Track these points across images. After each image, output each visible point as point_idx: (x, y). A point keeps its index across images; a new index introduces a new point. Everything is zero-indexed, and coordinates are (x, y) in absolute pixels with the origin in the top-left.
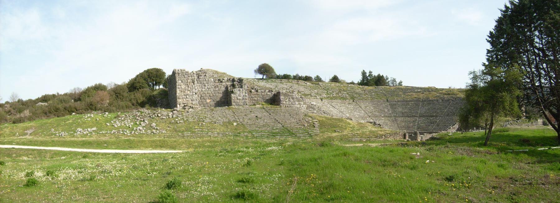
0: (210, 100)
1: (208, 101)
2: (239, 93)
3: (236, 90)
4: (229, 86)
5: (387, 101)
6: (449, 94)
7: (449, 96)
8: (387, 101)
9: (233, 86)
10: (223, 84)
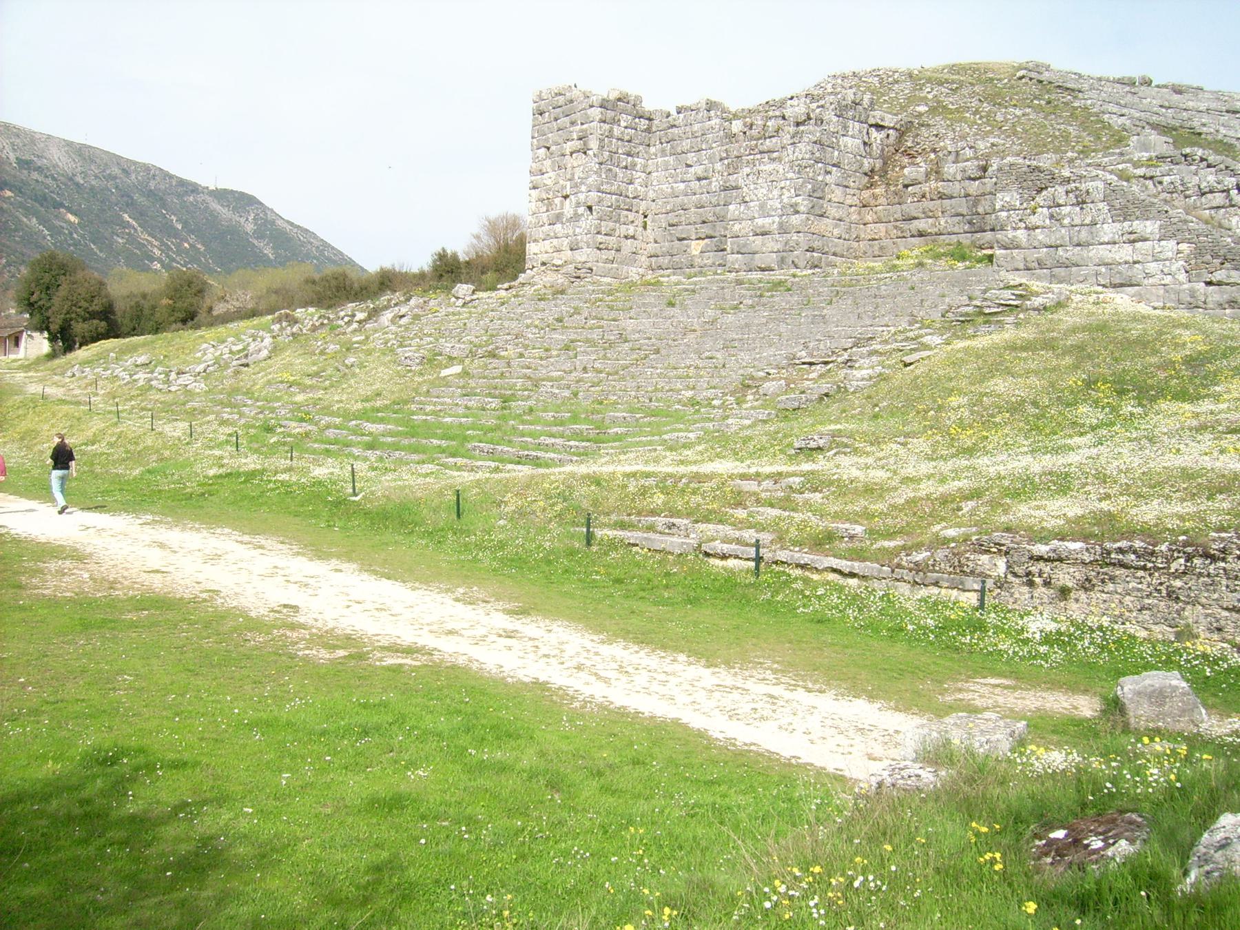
1: (696, 247)
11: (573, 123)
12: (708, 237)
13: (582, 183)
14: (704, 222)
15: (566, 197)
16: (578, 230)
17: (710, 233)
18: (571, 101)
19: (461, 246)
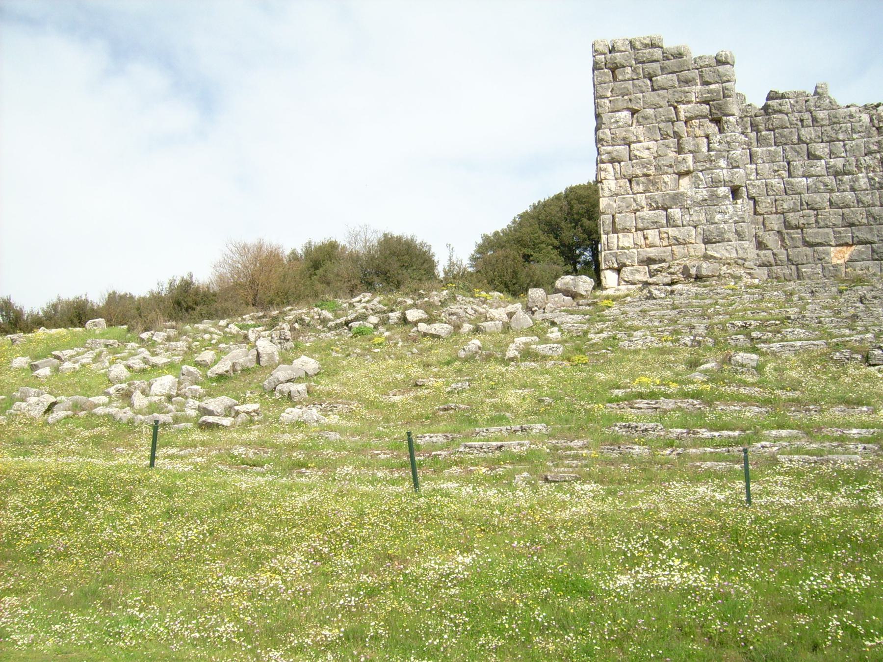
0: (848, 252)
1: (838, 256)
11: (687, 82)
12: (861, 243)
13: (718, 157)
14: (851, 225)
15: (681, 175)
16: (718, 217)
17: (869, 237)
18: (680, 55)
19: (204, 275)
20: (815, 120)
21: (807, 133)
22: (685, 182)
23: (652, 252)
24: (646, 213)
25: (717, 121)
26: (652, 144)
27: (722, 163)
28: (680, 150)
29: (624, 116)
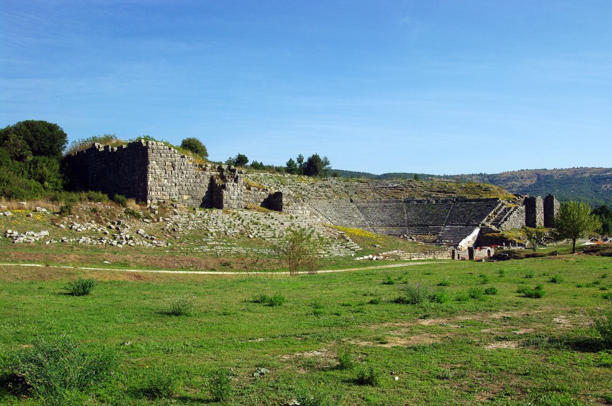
1: (185, 197)
2: (232, 188)
3: (230, 184)
4: (215, 177)
5: (352, 201)
6: (445, 192)
7: (445, 196)
8: (352, 201)
9: (222, 177)
10: (208, 173)
20: (184, 164)
21: (183, 167)
22: (166, 180)
23: (159, 197)
24: (158, 187)
25: (173, 167)
26: (160, 171)
27: (174, 178)
28: (166, 173)
29: (154, 162)
